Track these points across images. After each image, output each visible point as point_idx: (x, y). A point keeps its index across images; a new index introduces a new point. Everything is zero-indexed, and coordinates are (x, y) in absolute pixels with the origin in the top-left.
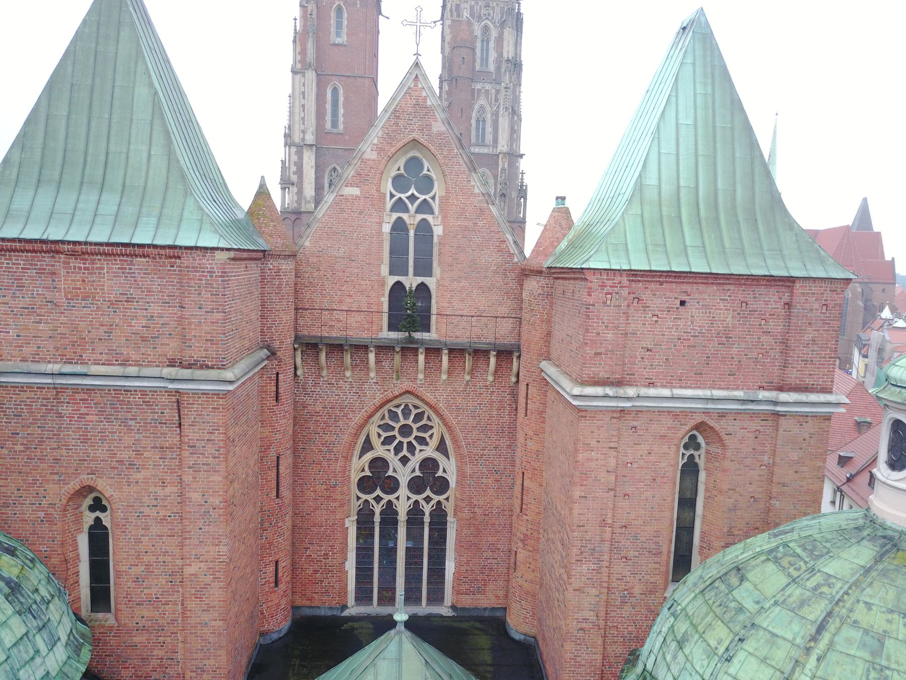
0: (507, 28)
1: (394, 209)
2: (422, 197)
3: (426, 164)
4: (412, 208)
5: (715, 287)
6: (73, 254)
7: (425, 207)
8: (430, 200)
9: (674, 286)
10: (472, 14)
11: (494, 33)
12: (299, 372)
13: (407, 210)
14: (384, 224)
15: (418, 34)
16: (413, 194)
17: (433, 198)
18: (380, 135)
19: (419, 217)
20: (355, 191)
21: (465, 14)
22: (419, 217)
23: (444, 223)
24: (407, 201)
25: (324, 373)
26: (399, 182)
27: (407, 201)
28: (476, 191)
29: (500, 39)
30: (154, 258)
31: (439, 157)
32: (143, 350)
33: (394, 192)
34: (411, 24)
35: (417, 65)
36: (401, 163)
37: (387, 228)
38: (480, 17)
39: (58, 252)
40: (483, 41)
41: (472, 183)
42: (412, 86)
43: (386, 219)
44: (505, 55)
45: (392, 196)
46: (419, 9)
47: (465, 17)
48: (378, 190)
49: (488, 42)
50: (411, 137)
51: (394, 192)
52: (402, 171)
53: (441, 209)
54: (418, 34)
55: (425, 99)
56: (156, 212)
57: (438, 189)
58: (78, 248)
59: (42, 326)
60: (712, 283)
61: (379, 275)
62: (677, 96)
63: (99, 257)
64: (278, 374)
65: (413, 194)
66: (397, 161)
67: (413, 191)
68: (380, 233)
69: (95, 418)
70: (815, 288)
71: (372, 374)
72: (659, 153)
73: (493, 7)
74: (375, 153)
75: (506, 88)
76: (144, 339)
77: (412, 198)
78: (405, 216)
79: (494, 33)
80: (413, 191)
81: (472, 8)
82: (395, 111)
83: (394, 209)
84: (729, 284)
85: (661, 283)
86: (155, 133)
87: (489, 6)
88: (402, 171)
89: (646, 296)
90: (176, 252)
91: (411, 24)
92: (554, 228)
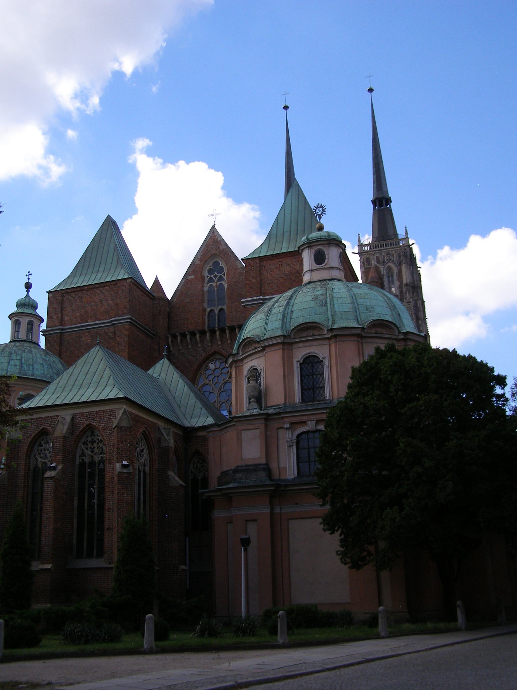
0: (404, 265)
1: (209, 282)
2: (219, 275)
3: (221, 263)
5: (291, 258)
6: (88, 290)
7: (221, 279)
8: (223, 275)
9: (276, 260)
10: (378, 262)
11: (395, 270)
12: (171, 349)
13: (213, 281)
14: (204, 288)
15: (215, 218)
16: (216, 274)
17: (224, 275)
18: (201, 255)
19: (219, 283)
20: (193, 277)
21: (373, 262)
22: (219, 283)
24: (213, 278)
25: (180, 348)
26: (210, 271)
27: (213, 278)
29: (400, 272)
30: (110, 286)
33: (208, 275)
35: (213, 227)
36: (211, 264)
37: (206, 289)
38: (384, 262)
39: (83, 290)
40: (388, 277)
41: (237, 264)
42: (212, 235)
43: (206, 285)
44: (405, 282)
45: (208, 277)
46: (214, 210)
47: (373, 264)
48: (201, 275)
49: (392, 276)
50: (213, 253)
51: (208, 275)
52: (211, 267)
54: (215, 218)
55: (217, 238)
56: (112, 275)
57: (225, 271)
58: (89, 287)
59: (77, 314)
60: (290, 256)
61: (203, 306)
62: (285, 206)
63: (94, 289)
64: (159, 343)
65: (216, 274)
66: (209, 263)
67: (216, 273)
68: (202, 290)
69: (90, 341)
71: (199, 345)
72: (277, 224)
73: (393, 255)
74: (199, 261)
75: (408, 302)
76: (106, 312)
78: (213, 284)
79: (395, 270)
80: (216, 273)
81: (377, 258)
82: (206, 245)
83: (209, 282)
84: (296, 255)
85: (272, 260)
86: (115, 255)
87: (389, 254)
88: (211, 267)
90: (116, 282)
91: (212, 215)
92: (317, 303)
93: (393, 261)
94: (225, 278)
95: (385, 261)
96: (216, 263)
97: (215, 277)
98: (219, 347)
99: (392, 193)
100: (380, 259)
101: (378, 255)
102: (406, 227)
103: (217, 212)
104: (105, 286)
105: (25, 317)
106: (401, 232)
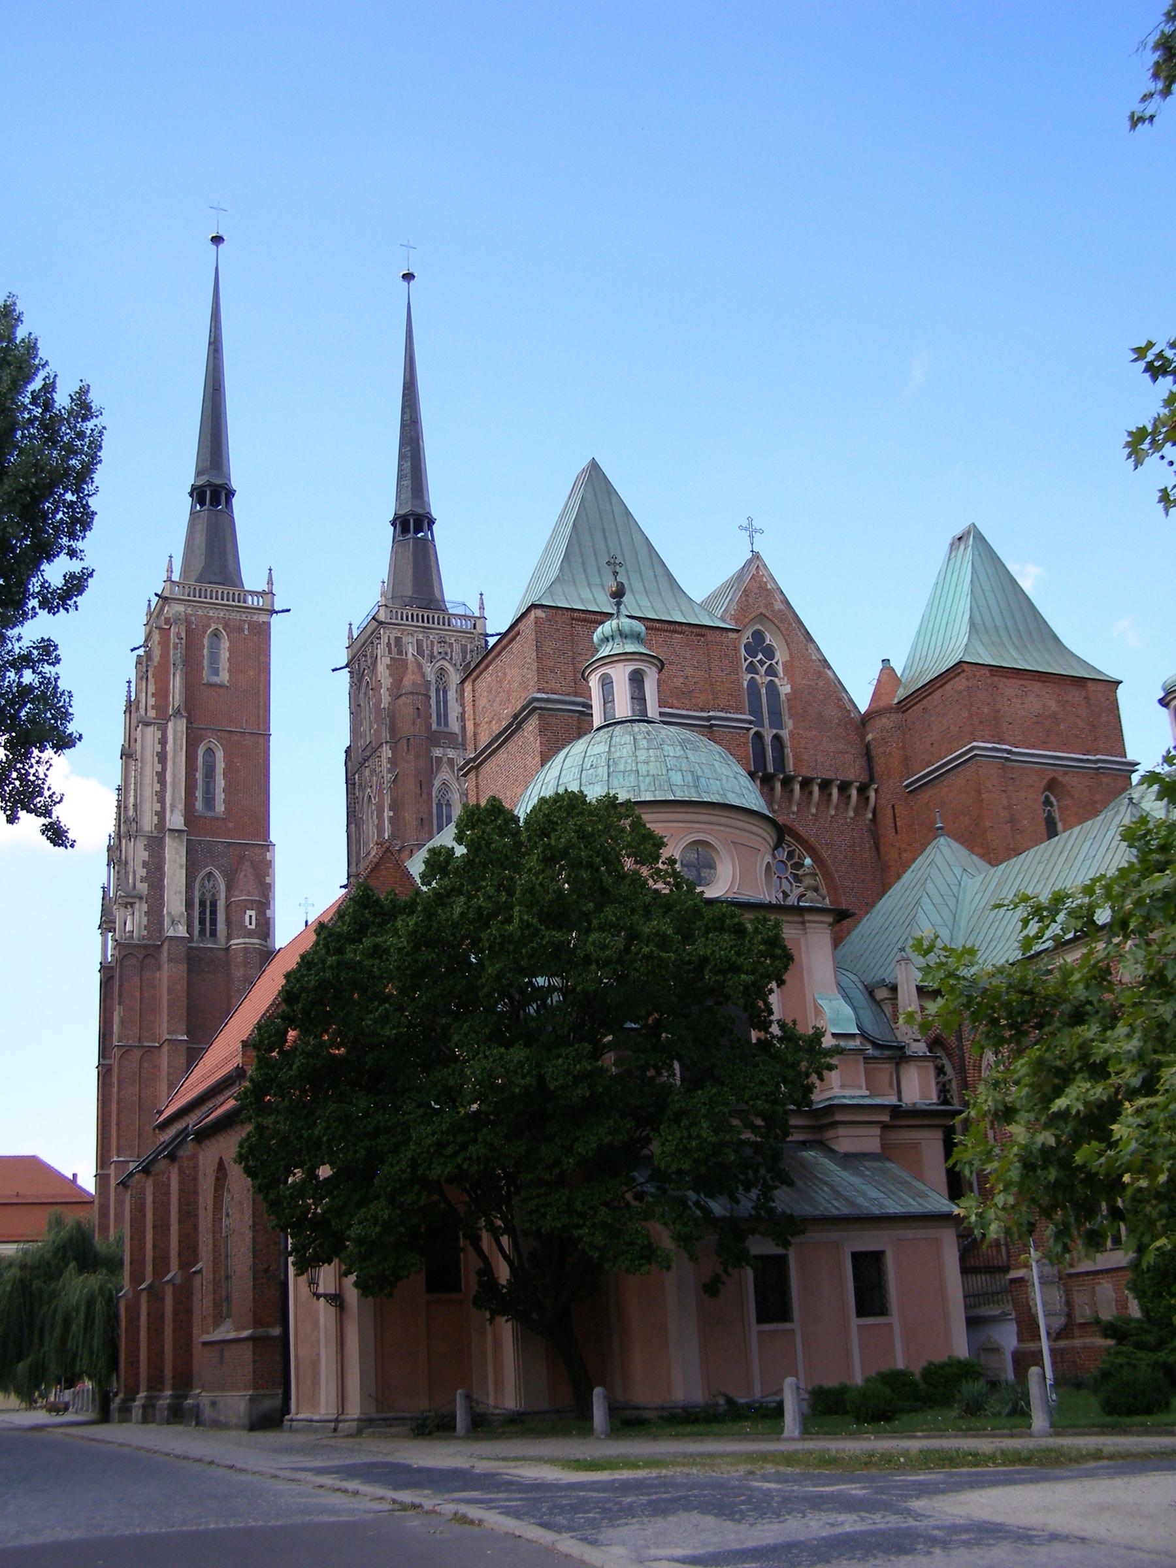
4: (762, 670)
7: (771, 671)
23: (792, 681)
28: (814, 658)
31: (783, 629)
32: (683, 701)
34: (746, 529)
37: (745, 683)
38: (432, 657)
45: (746, 660)
53: (786, 672)
55: (766, 583)
70: (1100, 687)
77: (761, 662)
80: (760, 656)
89: (1001, 685)
90: (703, 631)
93: (451, 659)
94: (780, 668)
95: (435, 654)
96: (758, 636)
97: (761, 662)
98: (791, 816)
99: (436, 509)
100: (425, 648)
101: (420, 637)
102: (270, 570)
103: (756, 525)
104: (675, 632)
105: (620, 665)
106: (252, 579)
